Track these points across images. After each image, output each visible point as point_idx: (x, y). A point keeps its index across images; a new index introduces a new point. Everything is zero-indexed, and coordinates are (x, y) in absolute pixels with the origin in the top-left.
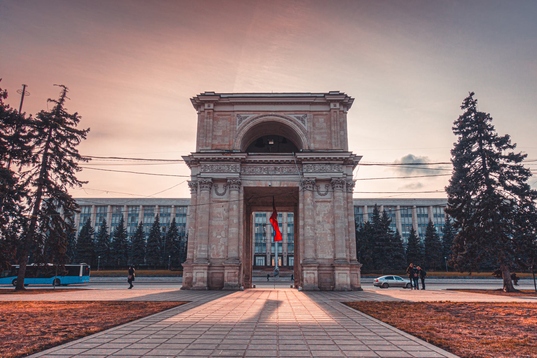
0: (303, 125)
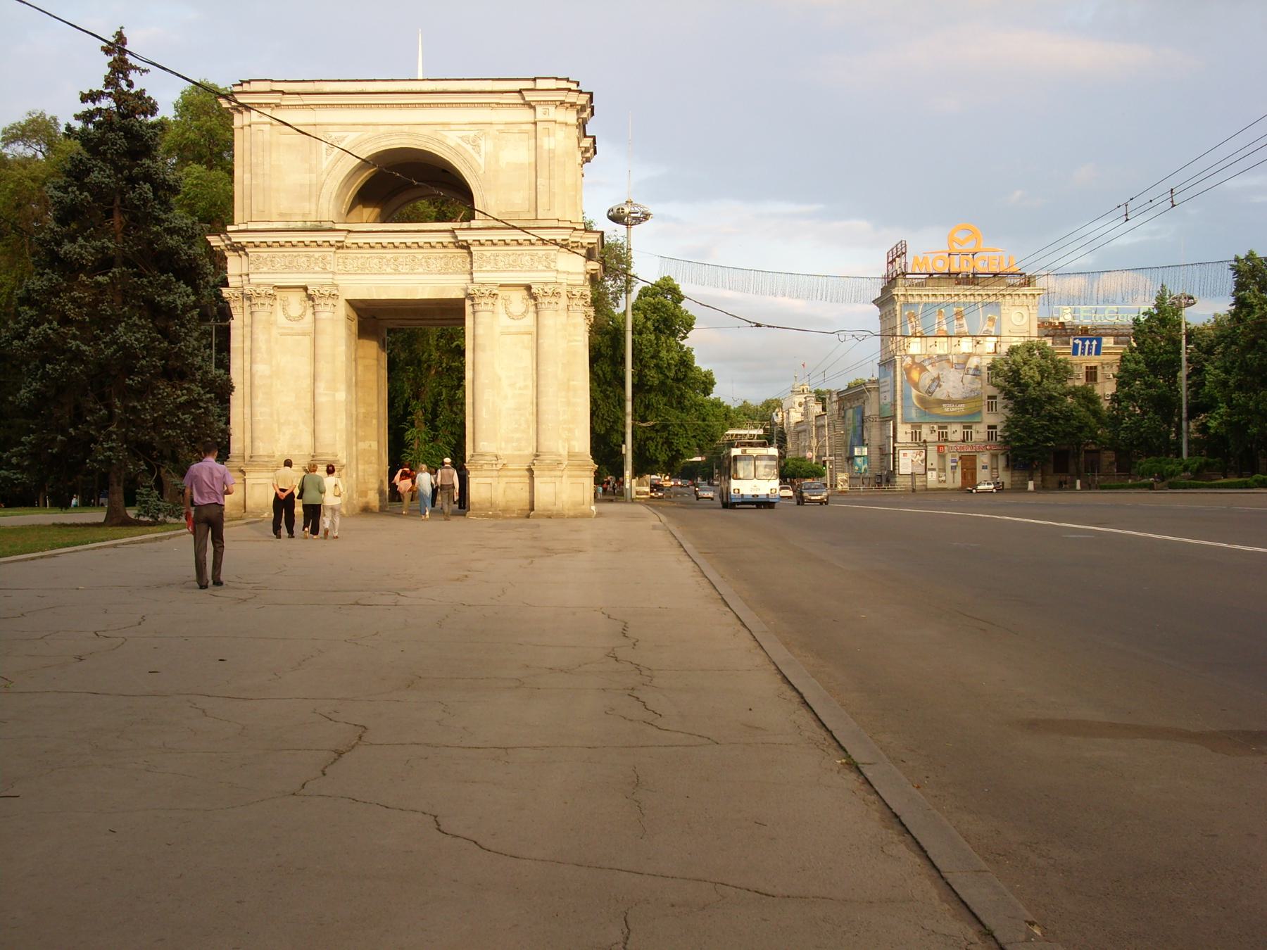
0: (476, 156)
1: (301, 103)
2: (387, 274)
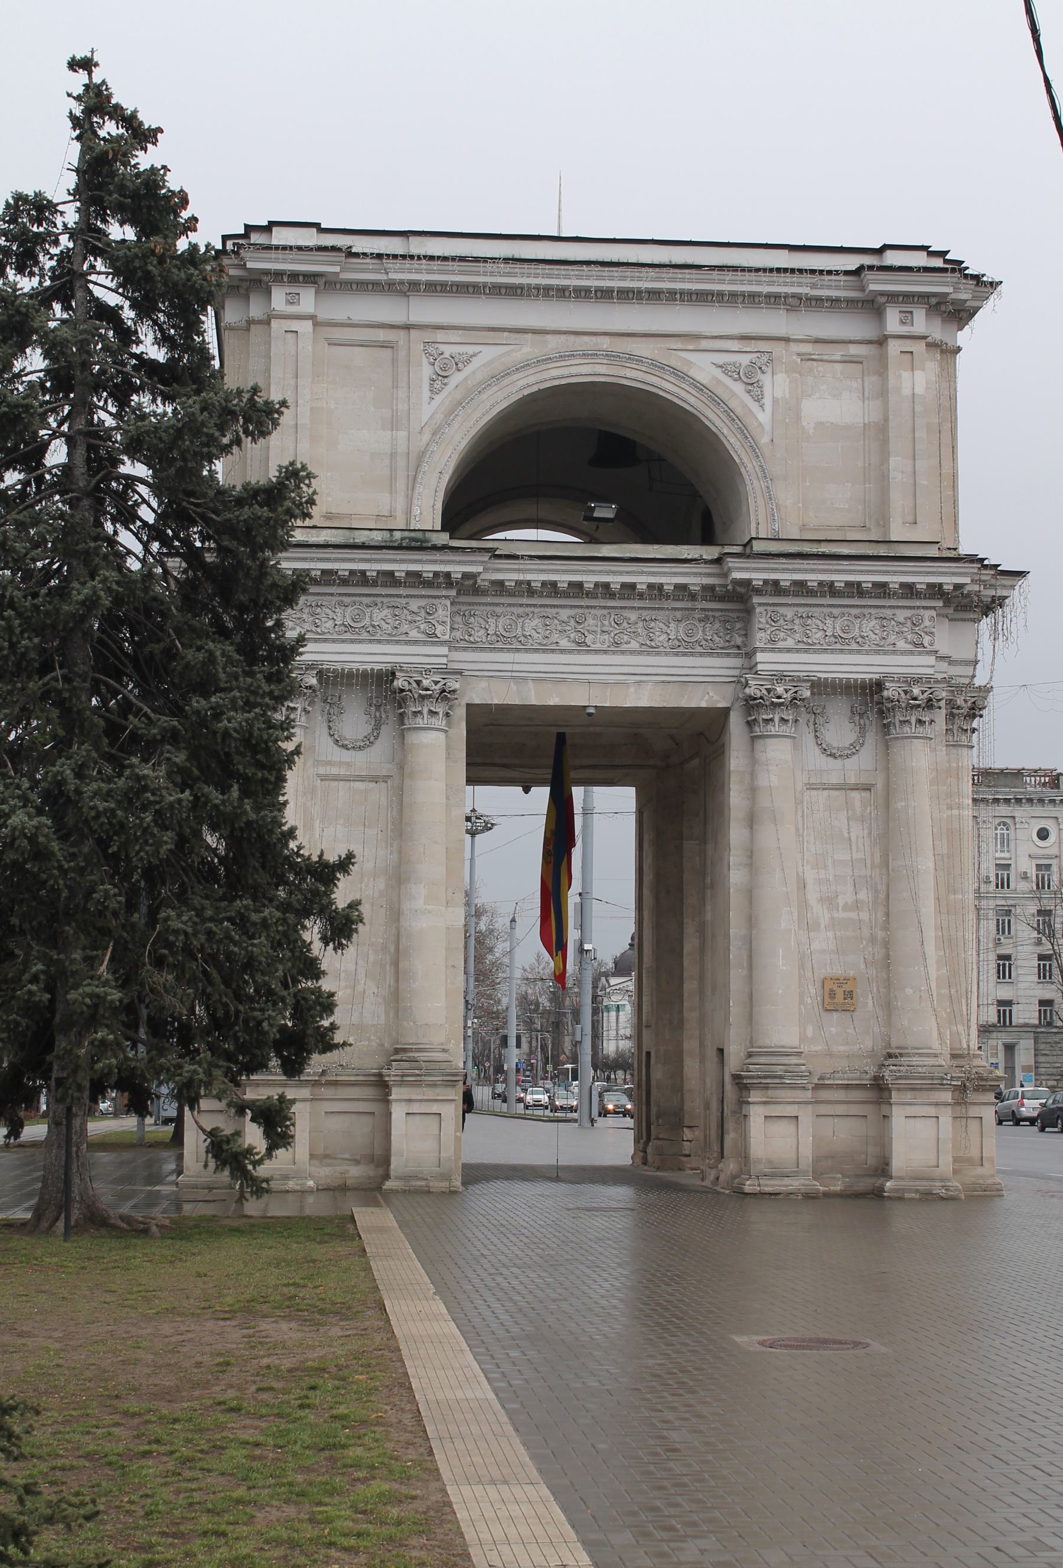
0: (754, 406)
1: (382, 277)
2: (562, 651)
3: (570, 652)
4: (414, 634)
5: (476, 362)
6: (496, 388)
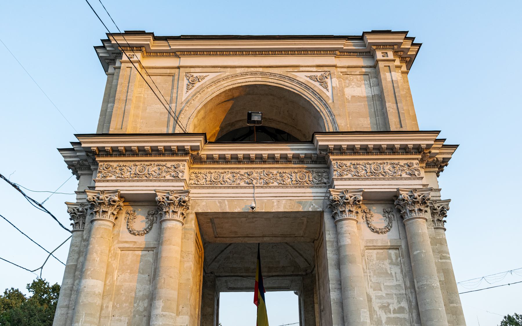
0: (324, 90)
2: (241, 187)
3: (245, 187)
4: (168, 177)
5: (206, 79)
6: (214, 87)
